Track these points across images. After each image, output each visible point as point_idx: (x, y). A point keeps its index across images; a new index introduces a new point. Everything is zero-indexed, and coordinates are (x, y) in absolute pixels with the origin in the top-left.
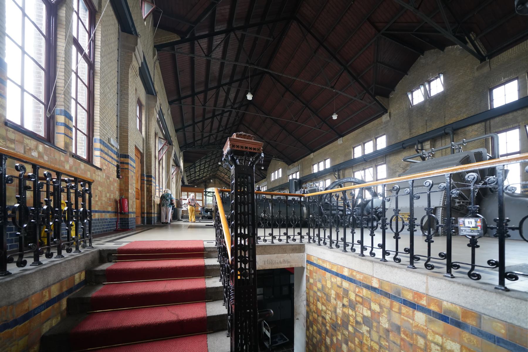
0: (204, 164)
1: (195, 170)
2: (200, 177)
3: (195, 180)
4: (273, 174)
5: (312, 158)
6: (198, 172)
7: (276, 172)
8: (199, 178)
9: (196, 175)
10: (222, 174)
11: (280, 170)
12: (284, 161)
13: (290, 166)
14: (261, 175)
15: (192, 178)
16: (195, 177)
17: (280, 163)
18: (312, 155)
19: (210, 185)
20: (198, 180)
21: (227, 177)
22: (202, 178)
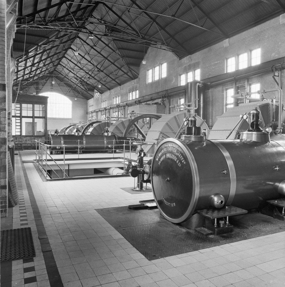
0: (40, 55)
1: (26, 64)
2: (31, 76)
4: (150, 71)
5: (226, 48)
6: (30, 68)
7: (157, 69)
8: (30, 77)
9: (26, 73)
10: (65, 69)
11: (165, 66)
12: (173, 51)
13: (186, 60)
14: (129, 74)
15: (19, 76)
16: (23, 76)
17: (170, 55)
18: (226, 43)
19: (45, 87)
20: (27, 80)
21: (73, 75)
22: (34, 76)
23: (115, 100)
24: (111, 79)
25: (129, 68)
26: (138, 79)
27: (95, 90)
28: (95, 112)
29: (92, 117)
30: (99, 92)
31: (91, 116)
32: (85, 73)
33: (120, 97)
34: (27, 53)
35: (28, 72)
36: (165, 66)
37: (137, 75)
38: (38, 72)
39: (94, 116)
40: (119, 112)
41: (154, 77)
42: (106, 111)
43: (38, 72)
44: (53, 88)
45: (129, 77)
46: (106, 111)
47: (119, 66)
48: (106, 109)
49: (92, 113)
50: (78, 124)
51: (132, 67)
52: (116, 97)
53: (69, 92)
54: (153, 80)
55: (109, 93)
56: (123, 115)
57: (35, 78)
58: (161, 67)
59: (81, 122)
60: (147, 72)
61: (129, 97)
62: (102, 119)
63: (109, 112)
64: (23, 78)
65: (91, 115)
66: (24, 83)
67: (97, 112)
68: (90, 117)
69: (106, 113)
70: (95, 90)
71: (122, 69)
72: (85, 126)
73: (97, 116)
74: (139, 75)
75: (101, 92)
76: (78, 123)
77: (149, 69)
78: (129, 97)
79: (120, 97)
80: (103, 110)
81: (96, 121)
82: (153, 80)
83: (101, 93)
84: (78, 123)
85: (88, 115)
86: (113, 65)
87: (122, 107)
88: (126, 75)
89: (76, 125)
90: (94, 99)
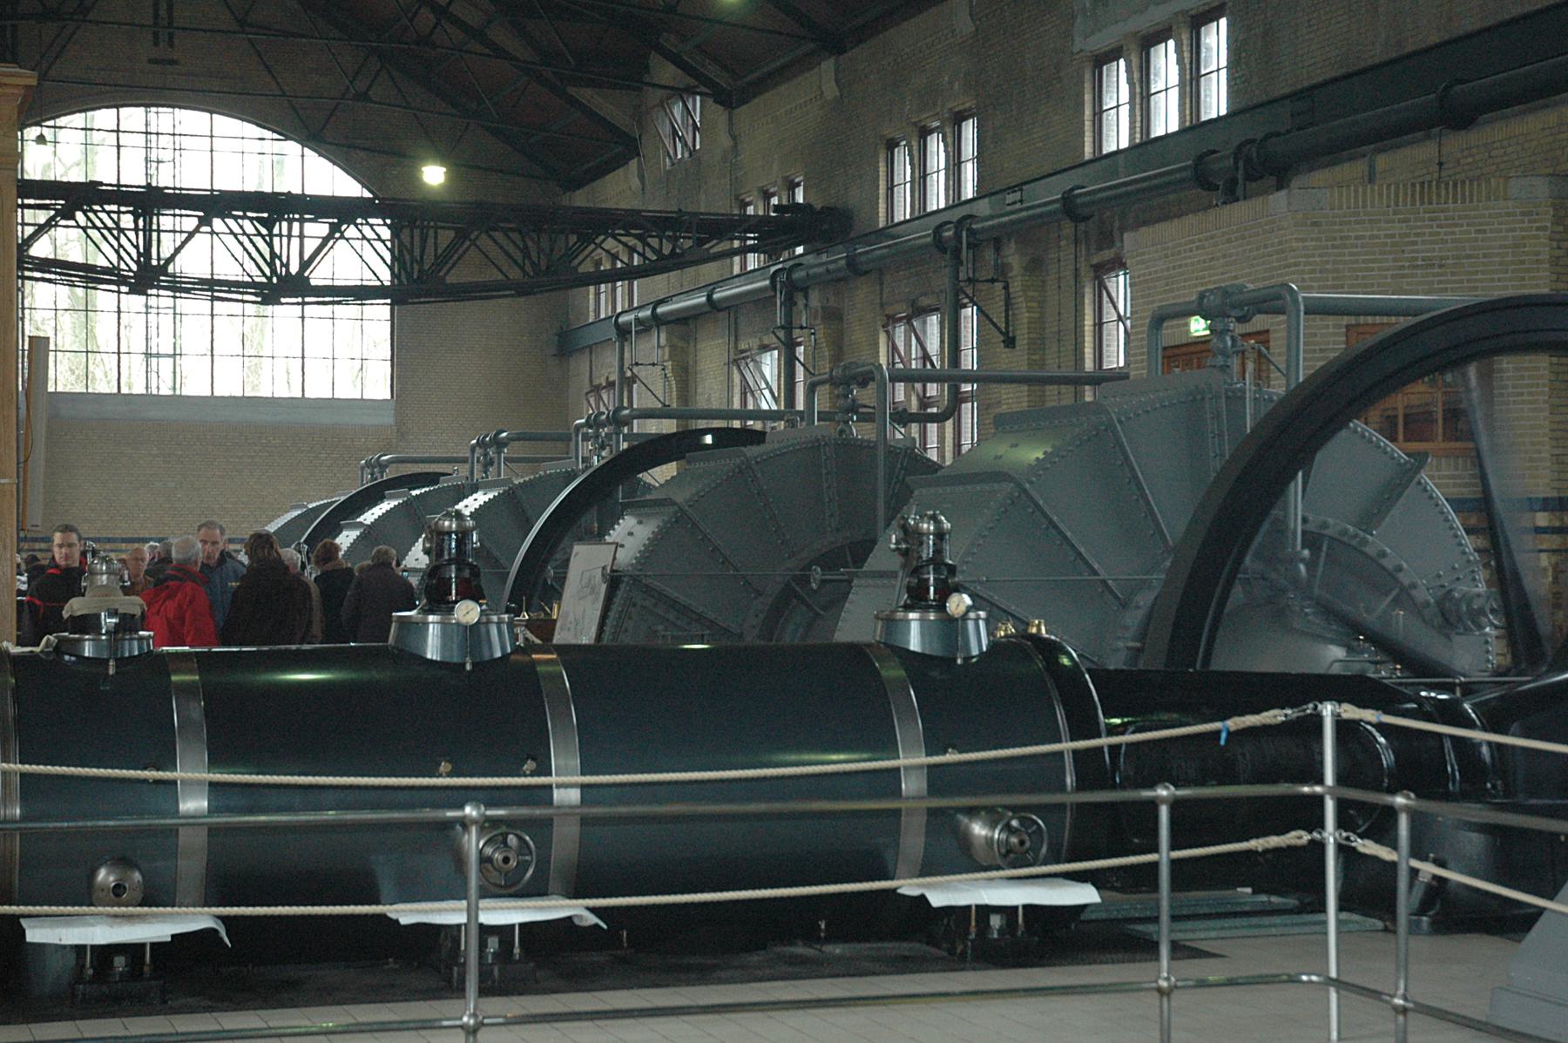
23: (904, 170)
27: (655, 59)
29: (628, 382)
31: (614, 377)
33: (969, 130)
40: (969, 314)
42: (790, 303)
44: (173, 62)
46: (790, 303)
48: (799, 275)
50: (463, 470)
52: (924, 133)
53: (363, 97)
55: (831, 90)
56: (1010, 342)
59: (499, 444)
61: (1088, 112)
62: (737, 405)
63: (833, 316)
65: (607, 367)
68: (596, 389)
69: (788, 327)
70: (655, 59)
72: (544, 487)
73: (685, 376)
75: (723, 80)
76: (464, 460)
78: (1088, 112)
79: (969, 130)
81: (669, 426)
83: (727, 99)
84: (464, 460)
87: (998, 244)
89: (432, 479)
90: (641, 177)
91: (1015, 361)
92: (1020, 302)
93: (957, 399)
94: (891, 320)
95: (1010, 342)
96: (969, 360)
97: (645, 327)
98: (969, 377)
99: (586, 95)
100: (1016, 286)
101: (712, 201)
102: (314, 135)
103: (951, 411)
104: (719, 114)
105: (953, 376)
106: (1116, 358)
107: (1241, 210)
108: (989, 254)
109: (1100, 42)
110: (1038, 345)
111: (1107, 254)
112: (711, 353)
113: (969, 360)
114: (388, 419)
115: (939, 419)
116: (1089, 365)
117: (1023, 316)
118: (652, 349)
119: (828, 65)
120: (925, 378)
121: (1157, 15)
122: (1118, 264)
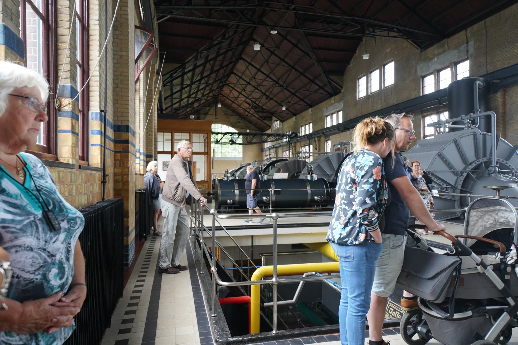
3: (180, 108)
11: (390, 68)
22: (193, 103)
24: (298, 99)
25: (328, 78)
26: (341, 95)
28: (274, 148)
29: (270, 155)
30: (279, 119)
32: (261, 94)
34: (183, 66)
35: (186, 95)
36: (390, 68)
37: (338, 89)
38: (199, 95)
39: (272, 154)
41: (371, 87)
43: (199, 95)
45: (326, 93)
46: (290, 145)
47: (311, 78)
49: (270, 149)
51: (332, 77)
53: (239, 122)
54: (369, 93)
55: (294, 120)
56: (316, 149)
57: (196, 105)
58: (383, 69)
60: (357, 81)
63: (295, 147)
64: (180, 104)
65: (267, 153)
66: (182, 112)
67: (277, 148)
69: (290, 148)
71: (316, 81)
73: (277, 153)
74: (342, 88)
77: (361, 76)
79: (311, 124)
80: (286, 145)
82: (369, 93)
85: (264, 153)
86: (302, 77)
88: (321, 91)
91: (317, 151)
92: (317, 145)
93: (310, 156)
94: (302, 147)
95: (316, 149)
96: (311, 151)
97: (272, 148)
98: (311, 153)
99: (265, 121)
100: (317, 143)
101: (280, 132)
102: (233, 126)
103: (309, 157)
104: (281, 123)
105: (309, 153)
106: (329, 151)
107: (343, 133)
108: (314, 139)
109: (327, 114)
110: (319, 150)
111: (328, 139)
112: (280, 150)
113: (311, 151)
114: (242, 159)
115: (308, 158)
116: (326, 152)
117: (318, 146)
118: (273, 151)
119: (294, 117)
120: (306, 153)
121: (333, 111)
122: (329, 140)
